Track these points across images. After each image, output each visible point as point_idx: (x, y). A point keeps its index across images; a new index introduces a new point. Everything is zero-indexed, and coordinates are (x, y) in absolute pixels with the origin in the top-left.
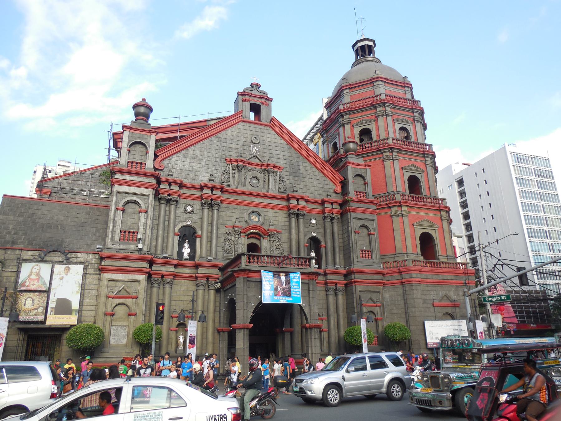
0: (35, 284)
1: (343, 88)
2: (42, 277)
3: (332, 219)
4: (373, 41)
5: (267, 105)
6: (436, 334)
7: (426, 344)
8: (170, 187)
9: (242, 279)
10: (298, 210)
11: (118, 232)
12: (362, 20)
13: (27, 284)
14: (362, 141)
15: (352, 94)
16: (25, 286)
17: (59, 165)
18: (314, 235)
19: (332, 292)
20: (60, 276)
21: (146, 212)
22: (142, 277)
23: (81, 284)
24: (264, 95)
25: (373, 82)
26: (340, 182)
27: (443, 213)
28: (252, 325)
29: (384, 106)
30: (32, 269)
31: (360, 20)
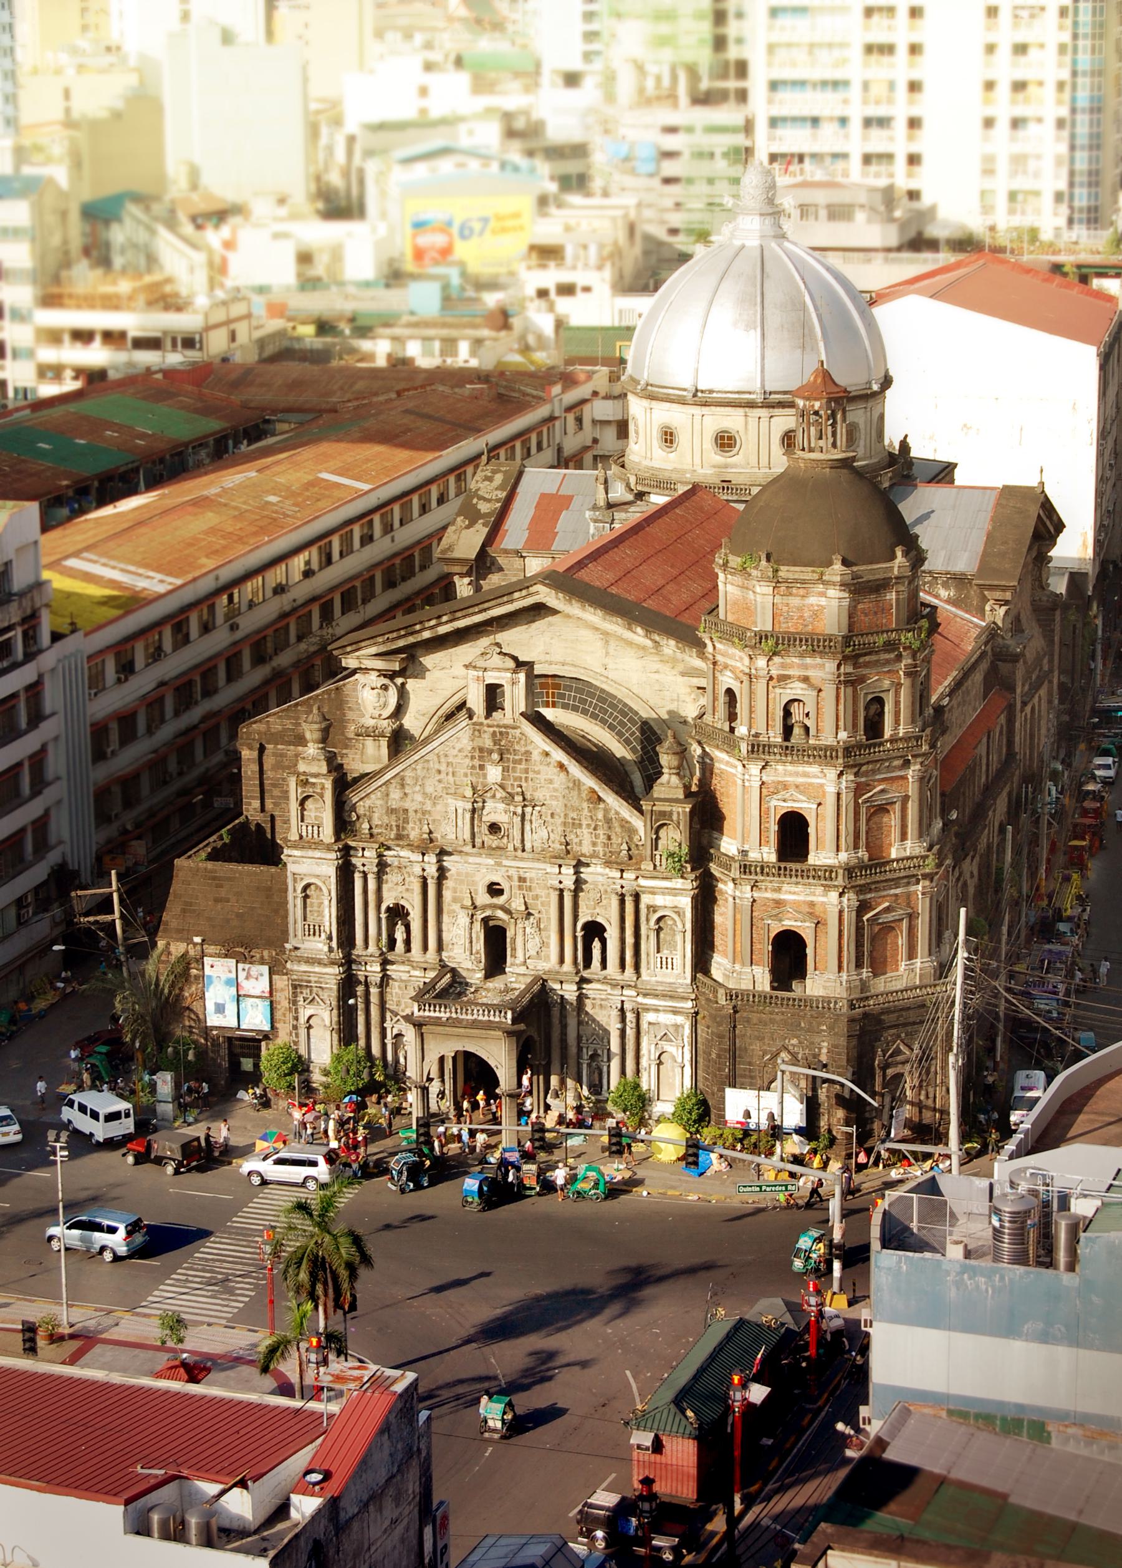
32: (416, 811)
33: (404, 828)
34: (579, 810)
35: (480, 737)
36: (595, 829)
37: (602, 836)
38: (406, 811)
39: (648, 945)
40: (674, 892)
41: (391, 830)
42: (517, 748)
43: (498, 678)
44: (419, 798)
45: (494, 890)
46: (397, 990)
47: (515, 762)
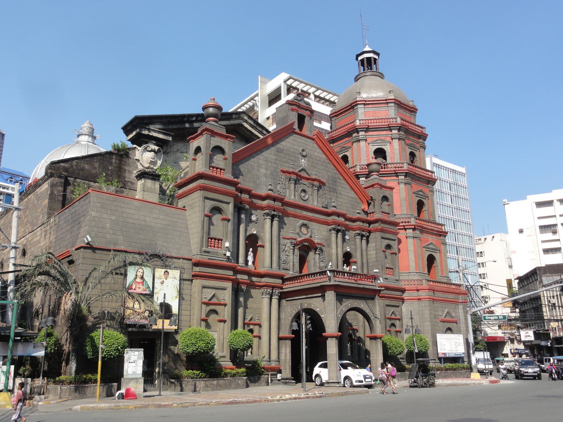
0: (140, 288)
1: (358, 103)
2: (146, 281)
4: (378, 54)
7: (438, 354)
10: (339, 226)
13: (134, 287)
15: (367, 110)
16: (131, 289)
18: (349, 250)
20: (161, 280)
22: (229, 285)
23: (179, 289)
24: (308, 106)
25: (388, 103)
30: (137, 272)
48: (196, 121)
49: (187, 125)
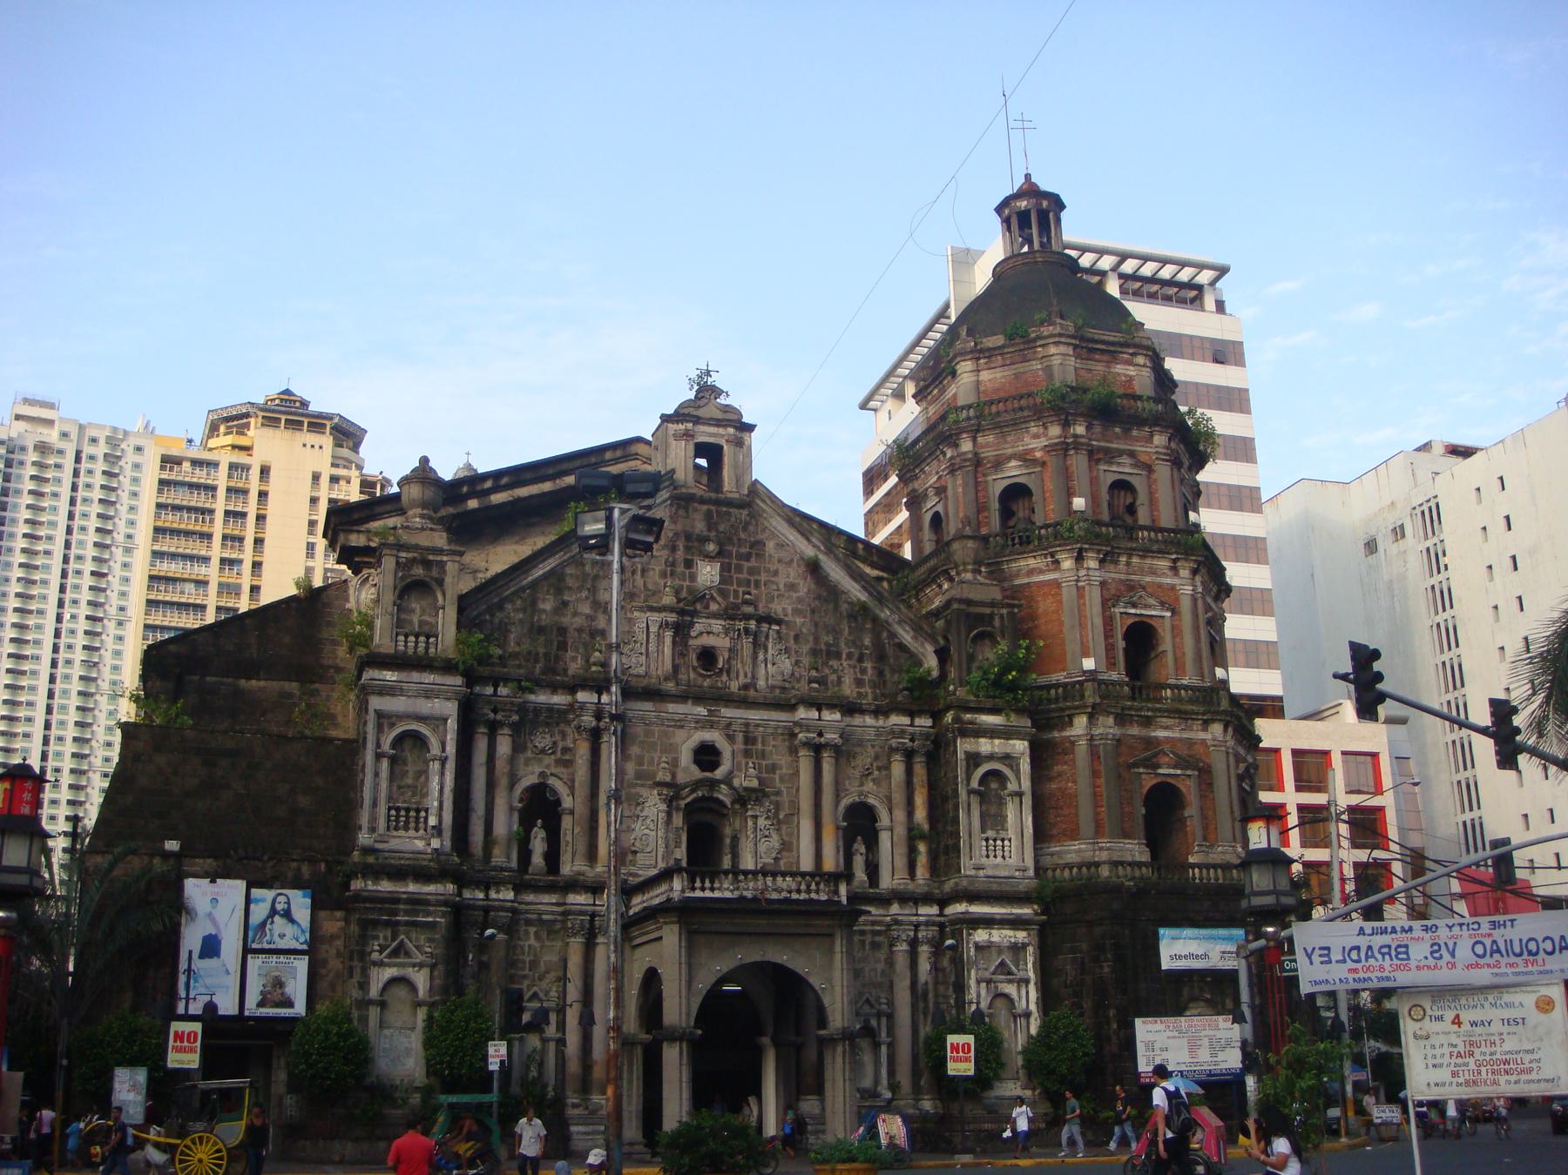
3: (909, 755)
5: (739, 443)
6: (1162, 1050)
8: (495, 690)
9: (676, 928)
11: (382, 809)
12: (1027, 125)
14: (1007, 513)
17: (18, 417)
19: (904, 947)
21: (443, 761)
26: (935, 652)
27: (1217, 729)
28: (699, 1032)
29: (1066, 425)
31: (1019, 124)
32: (580, 630)
33: (557, 658)
34: (836, 632)
35: (687, 517)
36: (861, 659)
37: (870, 671)
38: (562, 631)
39: (969, 818)
40: (1006, 733)
41: (537, 661)
42: (742, 536)
43: (714, 435)
44: (586, 609)
45: (706, 756)
46: (532, 941)
47: (740, 557)
48: (496, 489)
49: (473, 504)
